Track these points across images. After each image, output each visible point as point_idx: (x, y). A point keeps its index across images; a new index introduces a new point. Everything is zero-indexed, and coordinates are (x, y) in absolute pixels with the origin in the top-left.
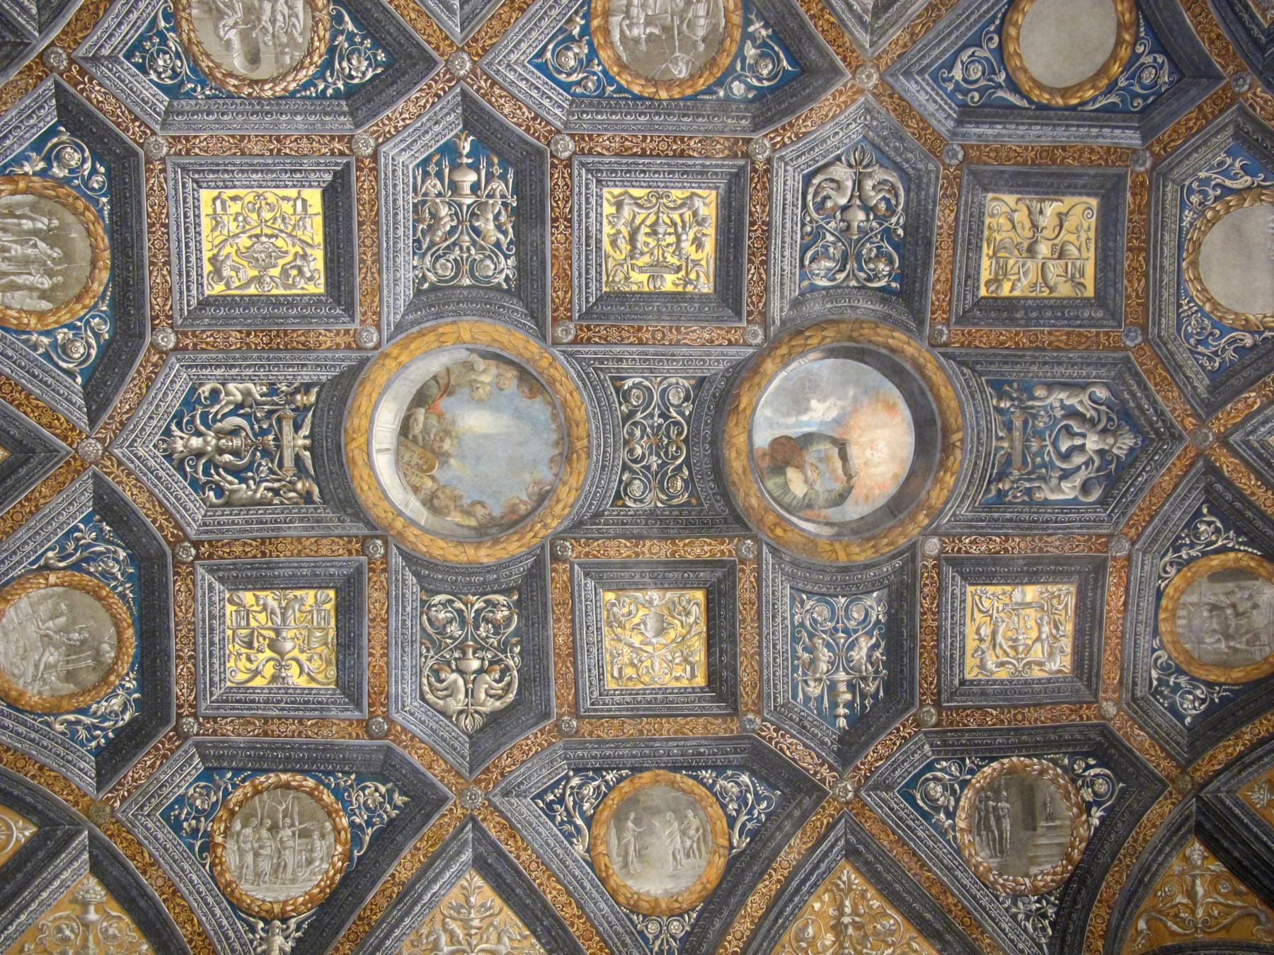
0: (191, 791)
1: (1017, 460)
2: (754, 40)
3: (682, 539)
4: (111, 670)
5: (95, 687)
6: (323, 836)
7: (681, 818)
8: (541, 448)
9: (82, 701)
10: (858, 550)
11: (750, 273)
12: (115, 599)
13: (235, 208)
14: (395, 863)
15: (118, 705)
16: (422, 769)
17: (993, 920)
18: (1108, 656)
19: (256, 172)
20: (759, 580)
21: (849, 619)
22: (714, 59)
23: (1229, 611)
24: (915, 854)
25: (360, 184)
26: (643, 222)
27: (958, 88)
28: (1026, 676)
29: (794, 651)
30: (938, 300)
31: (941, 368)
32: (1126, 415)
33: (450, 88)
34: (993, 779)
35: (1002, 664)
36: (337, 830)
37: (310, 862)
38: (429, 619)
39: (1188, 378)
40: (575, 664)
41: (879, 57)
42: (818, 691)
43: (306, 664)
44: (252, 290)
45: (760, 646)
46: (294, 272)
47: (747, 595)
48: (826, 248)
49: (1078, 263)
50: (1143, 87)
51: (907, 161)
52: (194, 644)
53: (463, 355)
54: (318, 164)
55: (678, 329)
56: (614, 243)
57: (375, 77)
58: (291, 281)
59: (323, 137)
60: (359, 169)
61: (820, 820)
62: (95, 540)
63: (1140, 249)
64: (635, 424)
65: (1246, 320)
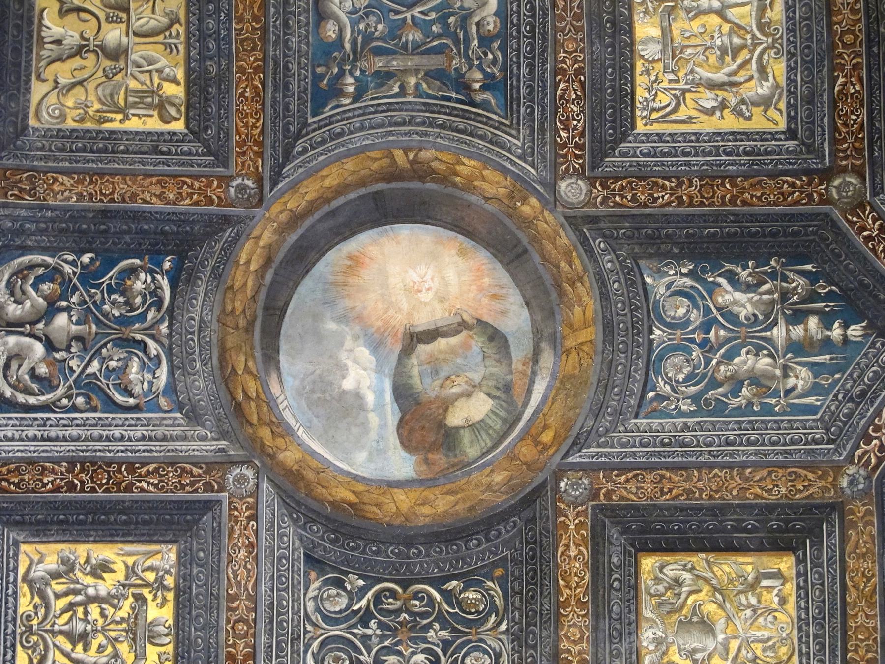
1: (435, 62)
3: (559, 591)
10: (578, 310)
11: (147, 489)
20: (623, 469)
21: (688, 322)
28: (782, 30)
30: (190, 195)
31: (294, 187)
35: (763, 71)
42: (804, 372)
45: (730, 467)
47: (649, 487)
48: (110, 371)
55: (232, 598)
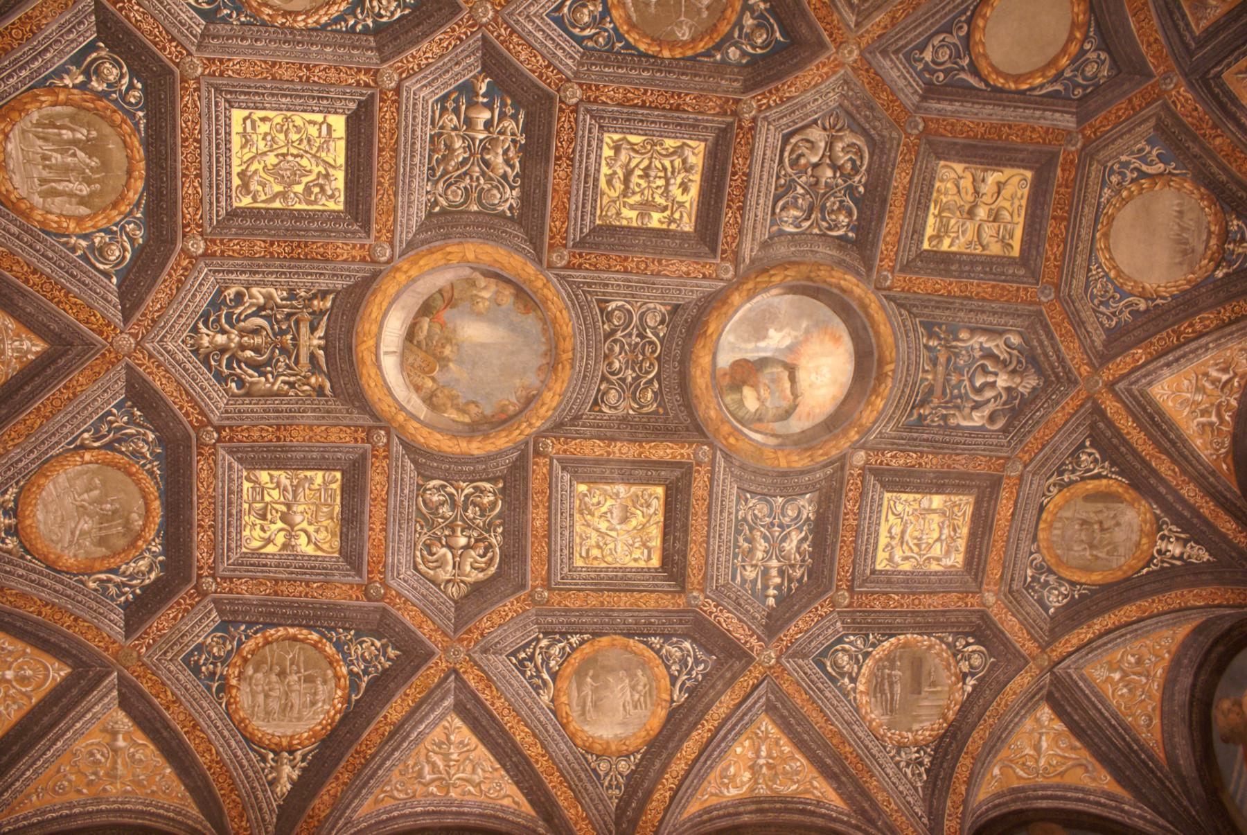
0: (209, 640)
1: (938, 390)
2: (752, 12)
3: (648, 442)
4: (139, 537)
5: (124, 551)
6: (325, 682)
7: (632, 676)
8: (531, 357)
9: (113, 562)
11: (728, 216)
12: (143, 475)
13: (264, 128)
14: (388, 706)
15: (145, 566)
16: (413, 628)
17: (880, 766)
18: (993, 556)
19: (286, 96)
20: (711, 480)
21: (784, 516)
22: (715, 25)
23: (1096, 527)
24: (822, 711)
25: (383, 114)
26: (637, 165)
27: (927, 68)
29: (736, 541)
31: (883, 307)
32: (1033, 360)
33: (472, 33)
34: (890, 652)
35: (906, 558)
36: (337, 677)
37: (313, 703)
38: (424, 501)
39: (1088, 332)
40: (549, 544)
41: (862, 36)
42: (753, 575)
43: (313, 535)
44: (277, 204)
45: (708, 536)
46: (317, 190)
47: (700, 493)
48: (796, 199)
49: (1009, 226)
50: (1085, 79)
51: (874, 128)
52: (214, 515)
53: (467, 272)
54: (345, 93)
55: (660, 262)
56: (609, 182)
57: (402, 17)
58: (313, 198)
59: (350, 68)
60: (382, 100)
61: (746, 681)
62: (127, 423)
63: (1063, 219)
64: (615, 341)
65: (1143, 288)
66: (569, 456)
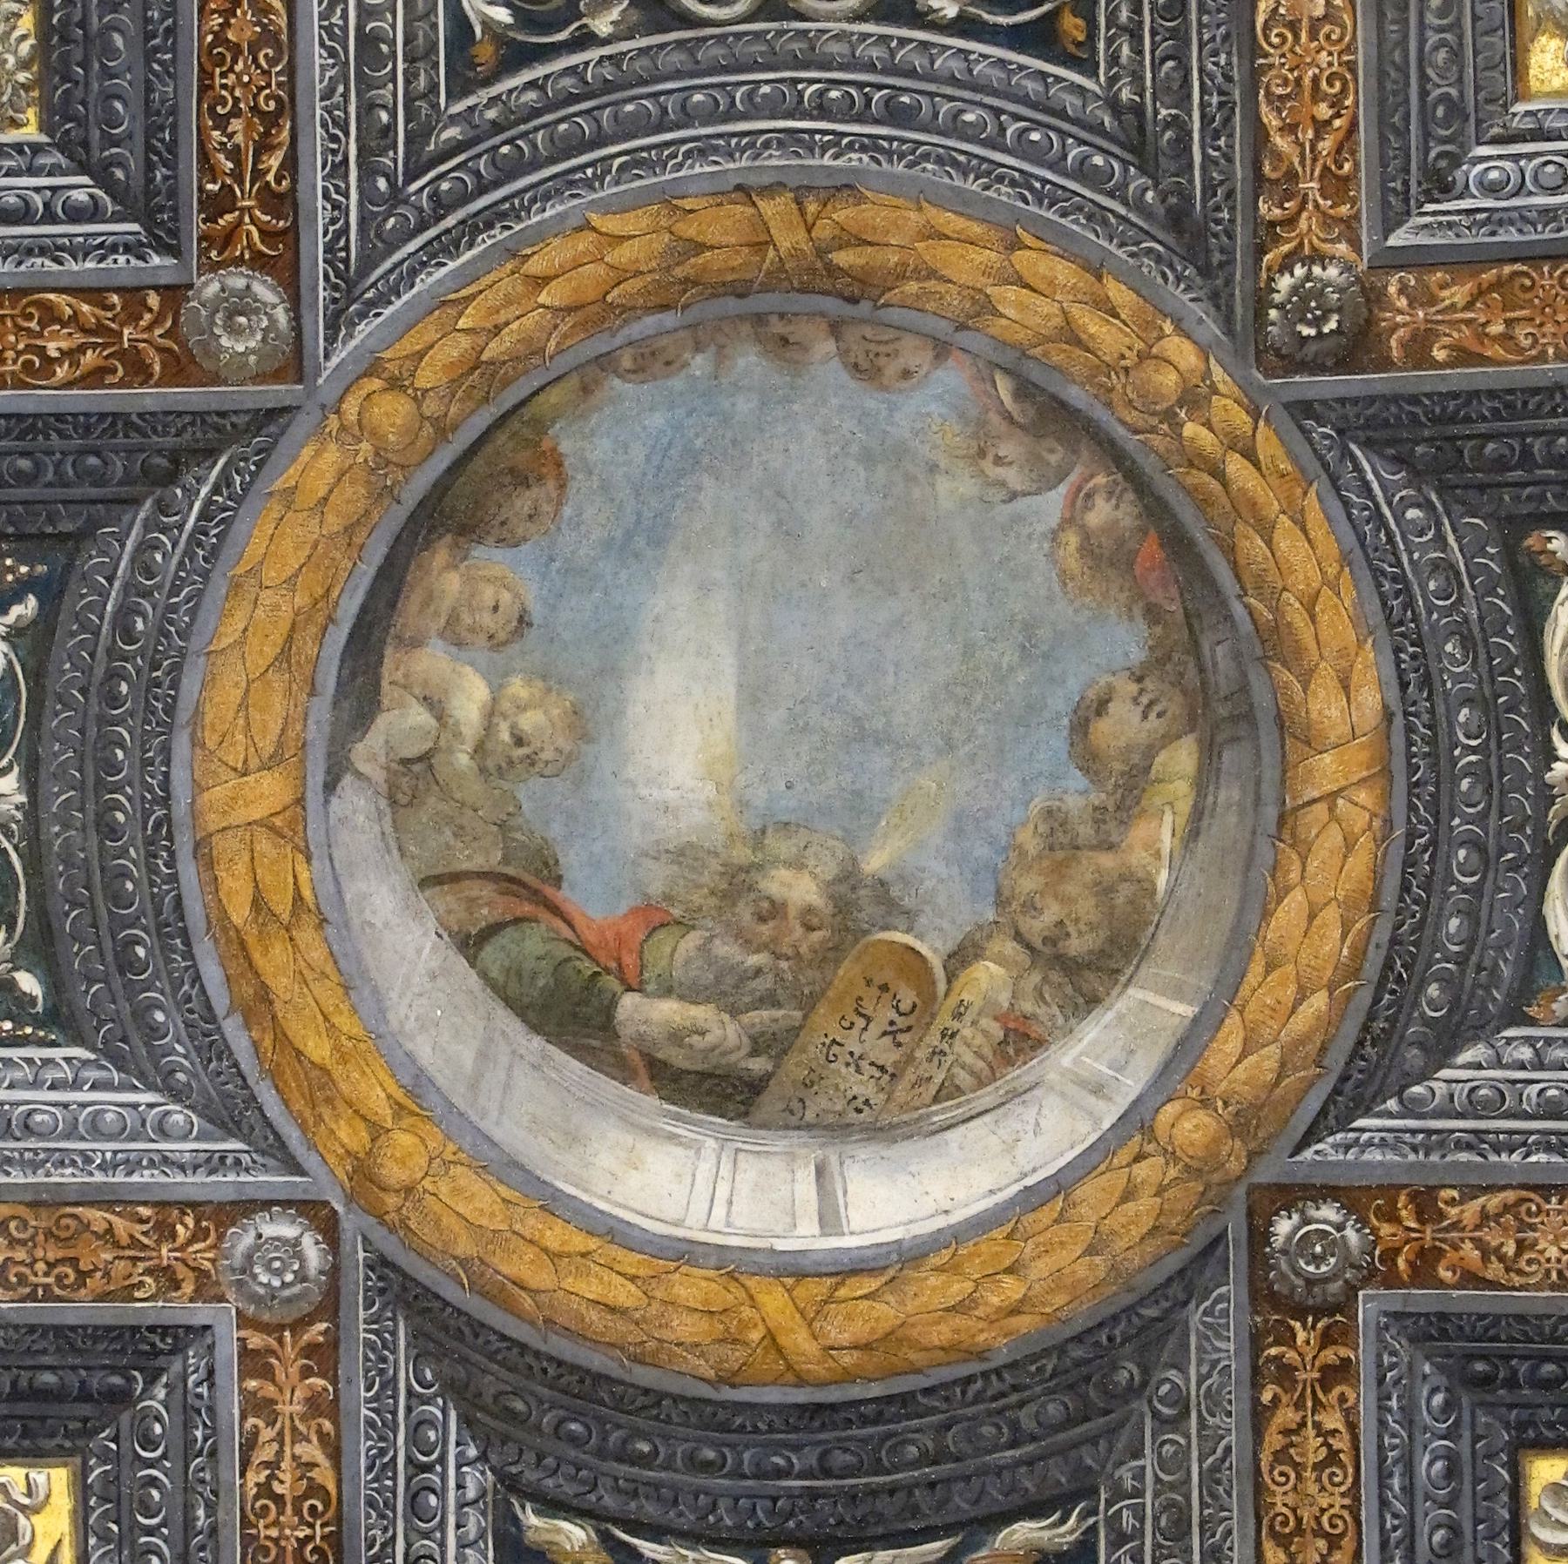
8: (808, 427)
53: (356, 811)
66: (1362, 162)
